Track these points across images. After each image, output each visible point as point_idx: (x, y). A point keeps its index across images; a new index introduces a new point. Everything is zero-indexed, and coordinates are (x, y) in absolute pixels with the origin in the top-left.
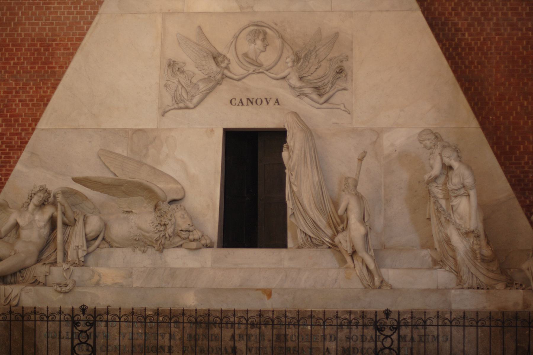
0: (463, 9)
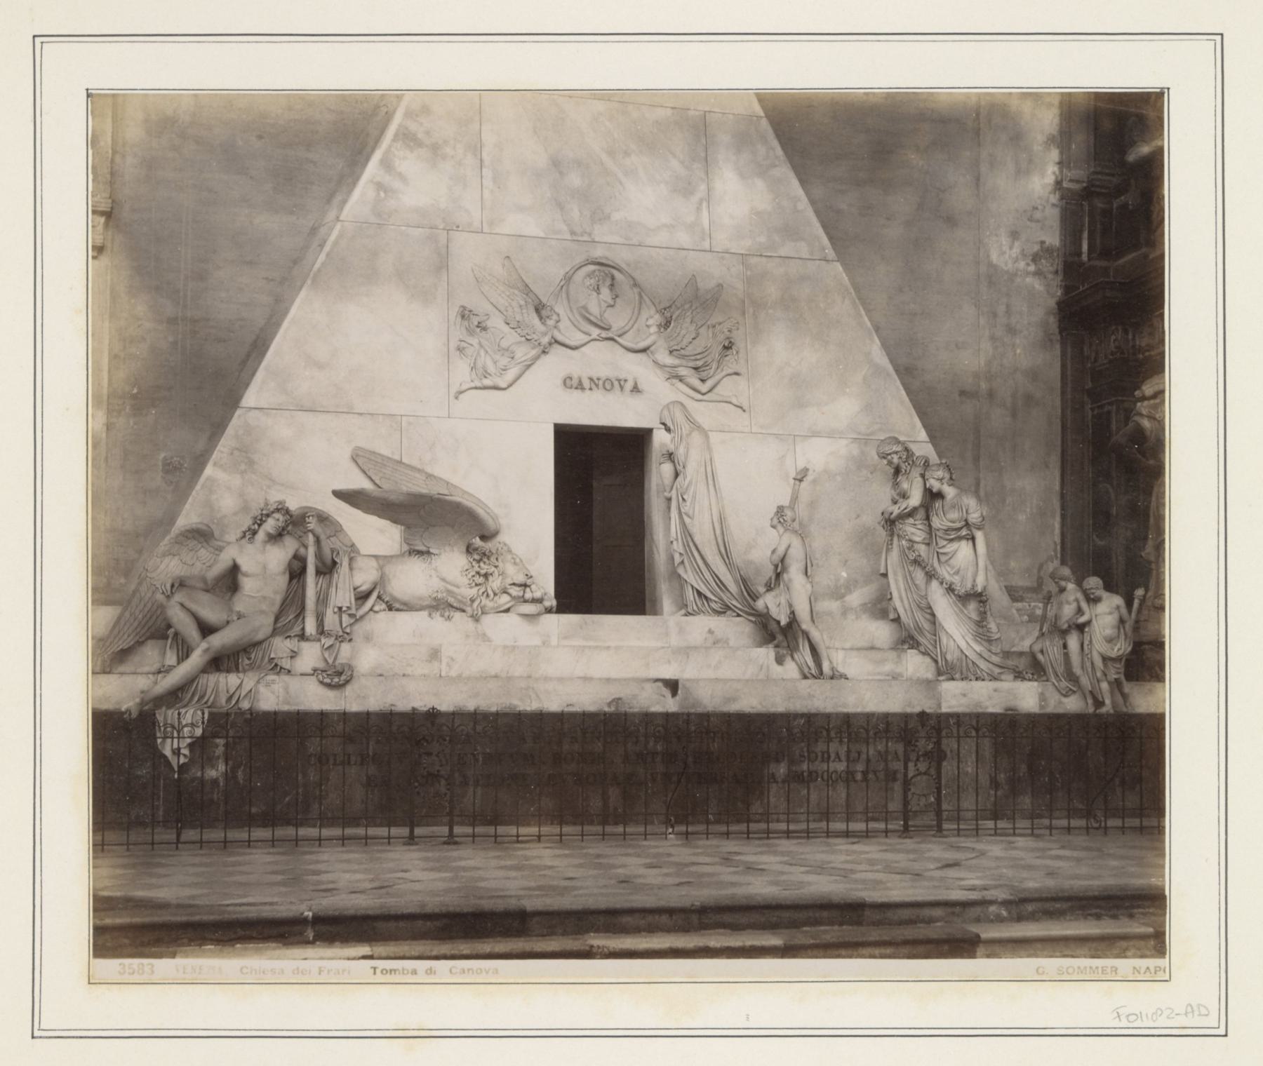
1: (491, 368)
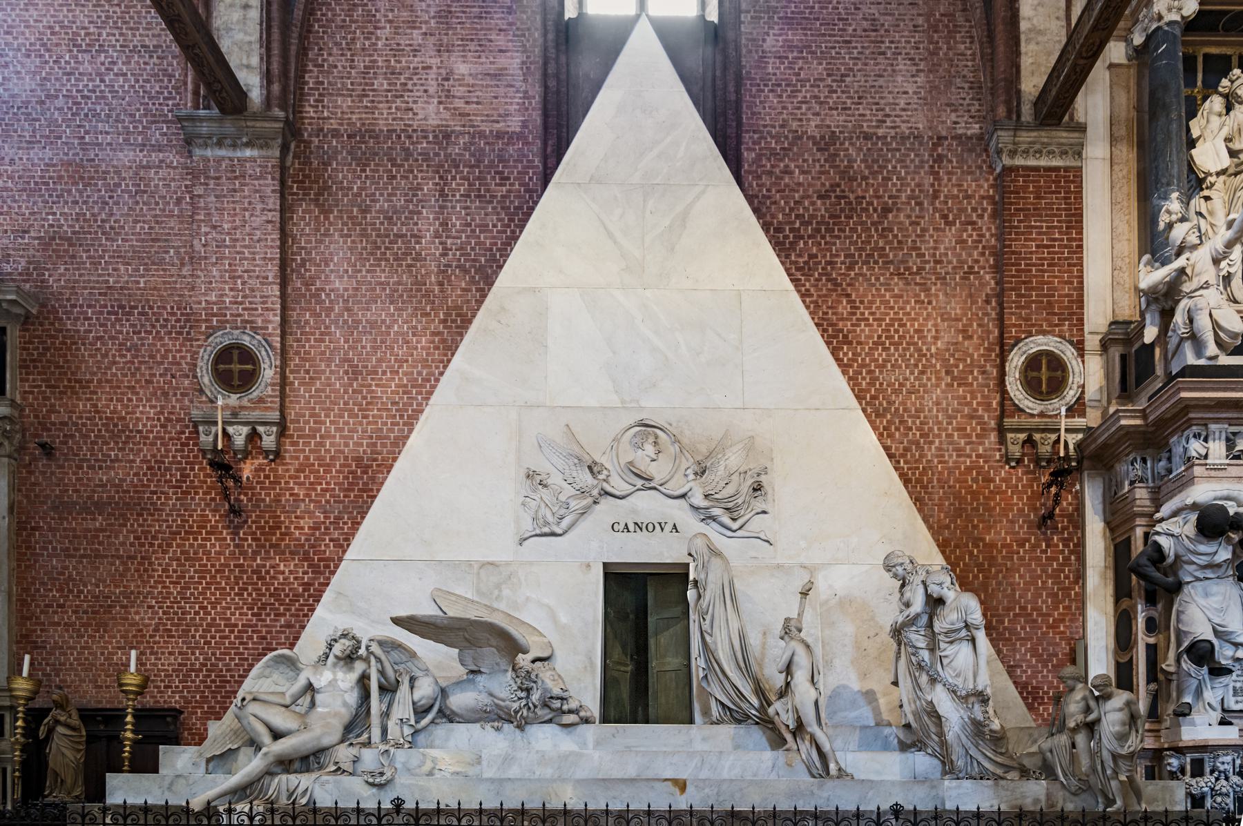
0: (897, 429)
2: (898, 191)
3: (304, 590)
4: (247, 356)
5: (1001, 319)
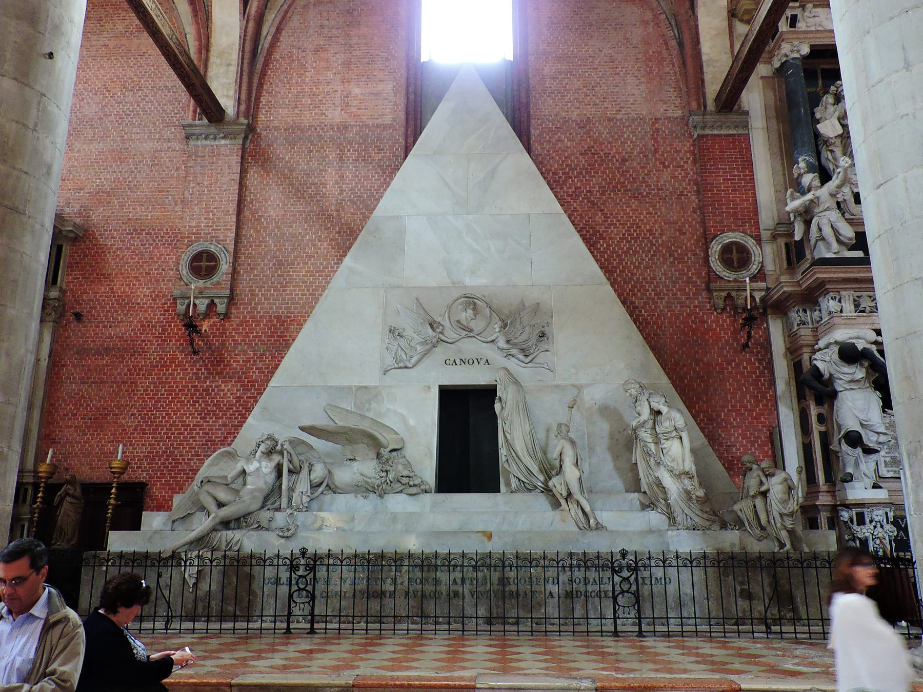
0: (639, 291)
1: (405, 358)
2: (631, 149)
3: (237, 402)
4: (211, 257)
5: (703, 223)
